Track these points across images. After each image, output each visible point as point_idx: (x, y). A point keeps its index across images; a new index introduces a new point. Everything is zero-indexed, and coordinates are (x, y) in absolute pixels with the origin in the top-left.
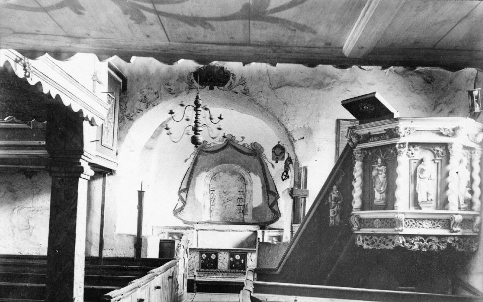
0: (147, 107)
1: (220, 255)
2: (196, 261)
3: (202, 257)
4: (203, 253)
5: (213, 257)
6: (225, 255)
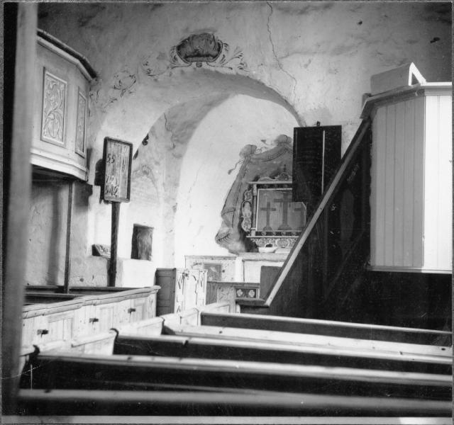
0: (122, 94)
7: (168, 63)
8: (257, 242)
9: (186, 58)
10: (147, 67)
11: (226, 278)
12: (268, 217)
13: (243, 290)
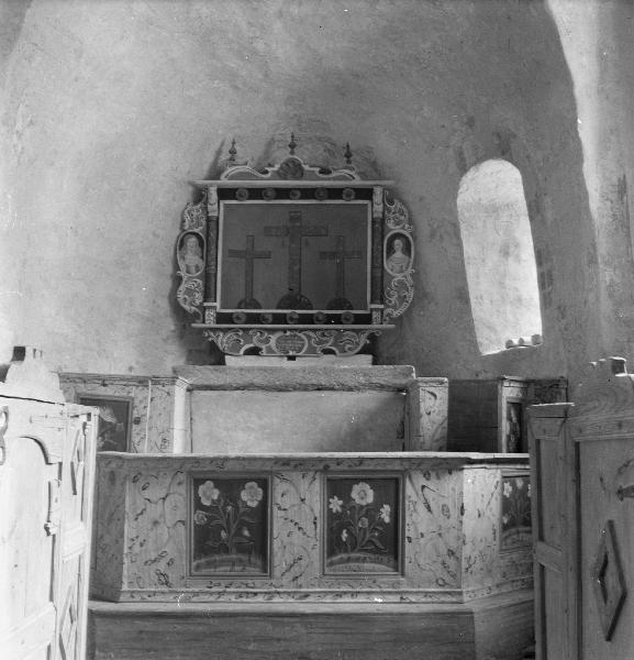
1: (279, 487)
2: (170, 519)
3: (198, 499)
4: (203, 481)
5: (250, 497)
6: (304, 485)
8: (222, 341)
11: (144, 446)
12: (250, 273)
13: (218, 483)
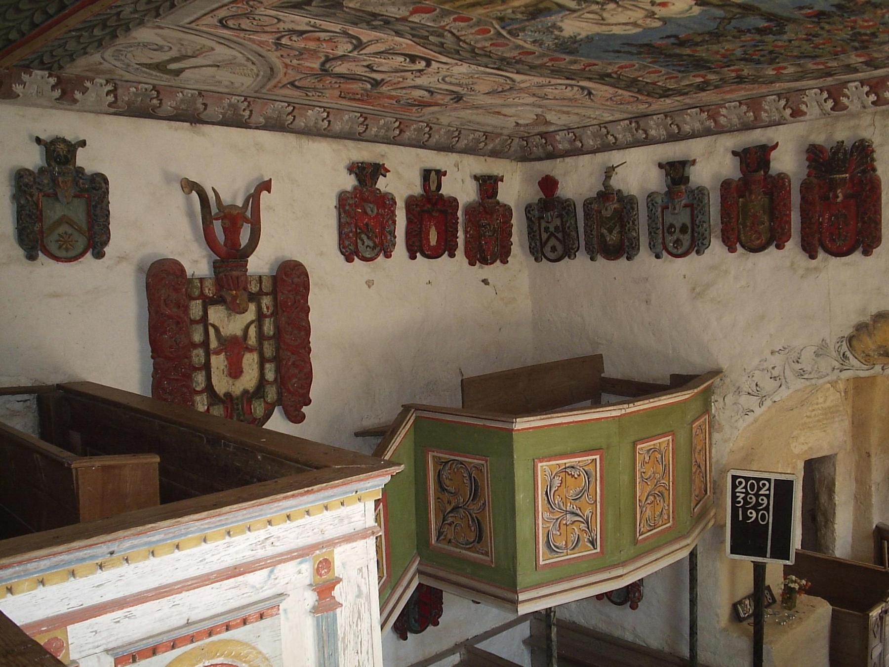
0: (761, 404)
7: (836, 364)
9: (867, 359)
10: (799, 366)
